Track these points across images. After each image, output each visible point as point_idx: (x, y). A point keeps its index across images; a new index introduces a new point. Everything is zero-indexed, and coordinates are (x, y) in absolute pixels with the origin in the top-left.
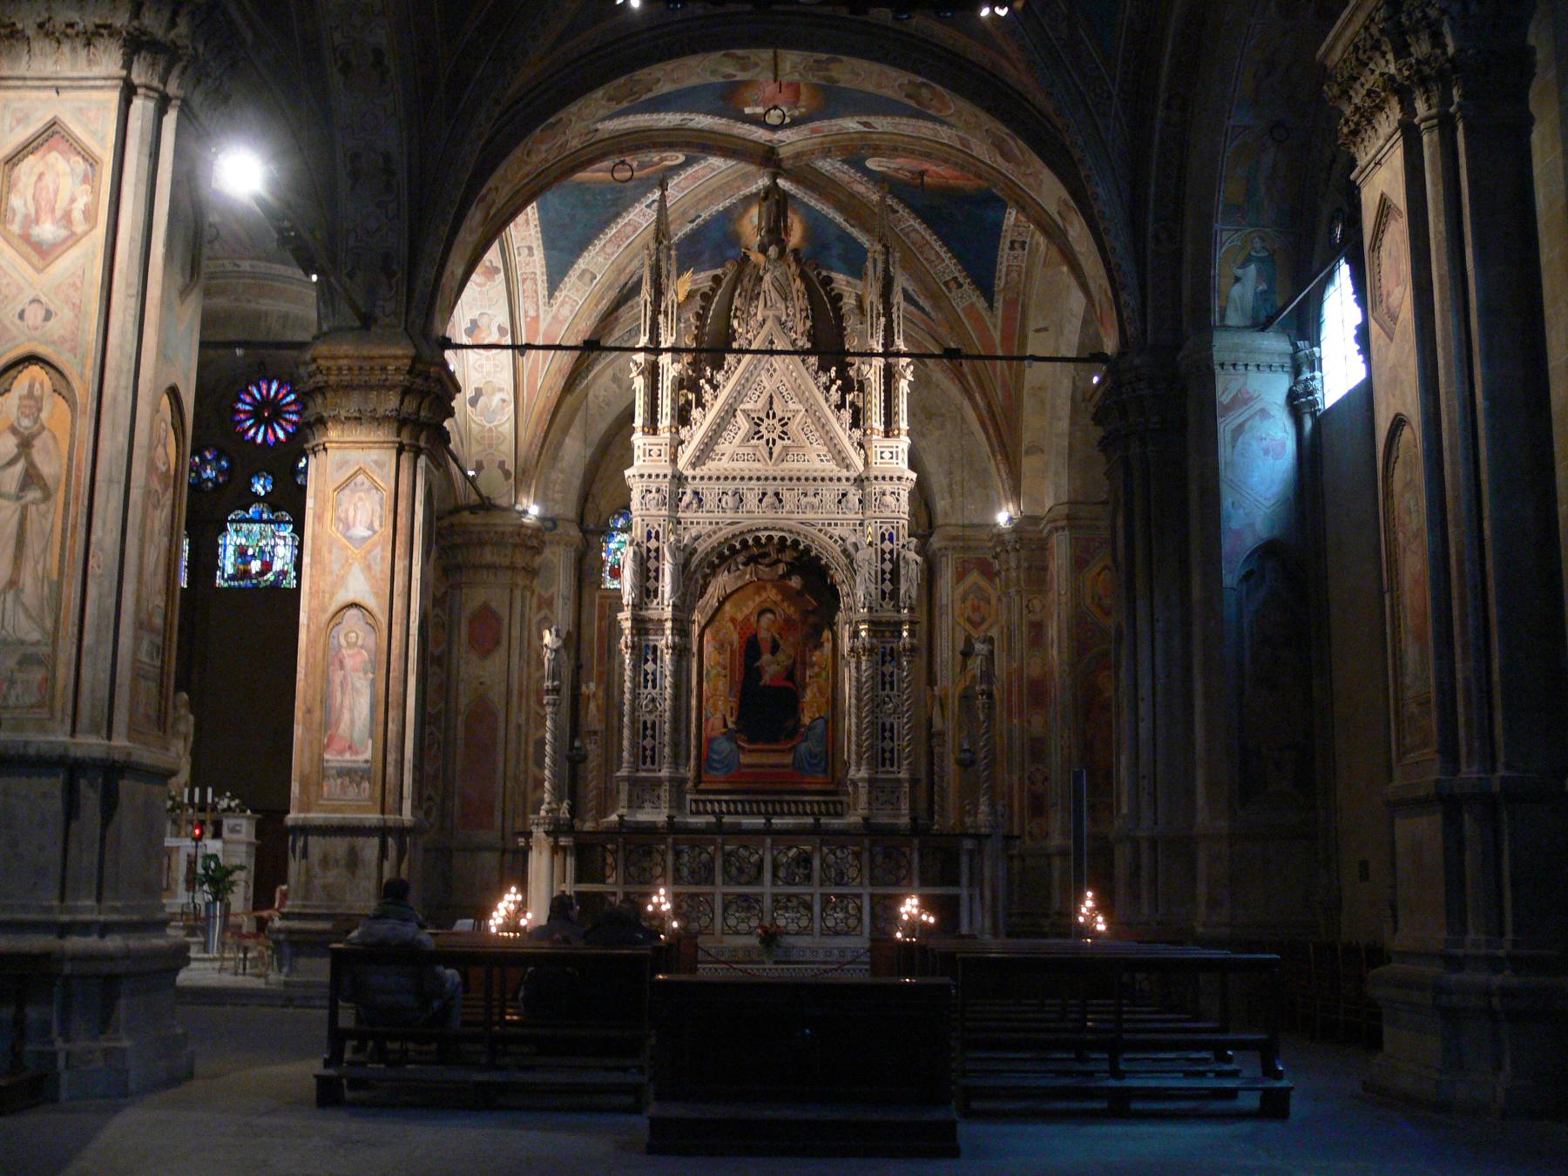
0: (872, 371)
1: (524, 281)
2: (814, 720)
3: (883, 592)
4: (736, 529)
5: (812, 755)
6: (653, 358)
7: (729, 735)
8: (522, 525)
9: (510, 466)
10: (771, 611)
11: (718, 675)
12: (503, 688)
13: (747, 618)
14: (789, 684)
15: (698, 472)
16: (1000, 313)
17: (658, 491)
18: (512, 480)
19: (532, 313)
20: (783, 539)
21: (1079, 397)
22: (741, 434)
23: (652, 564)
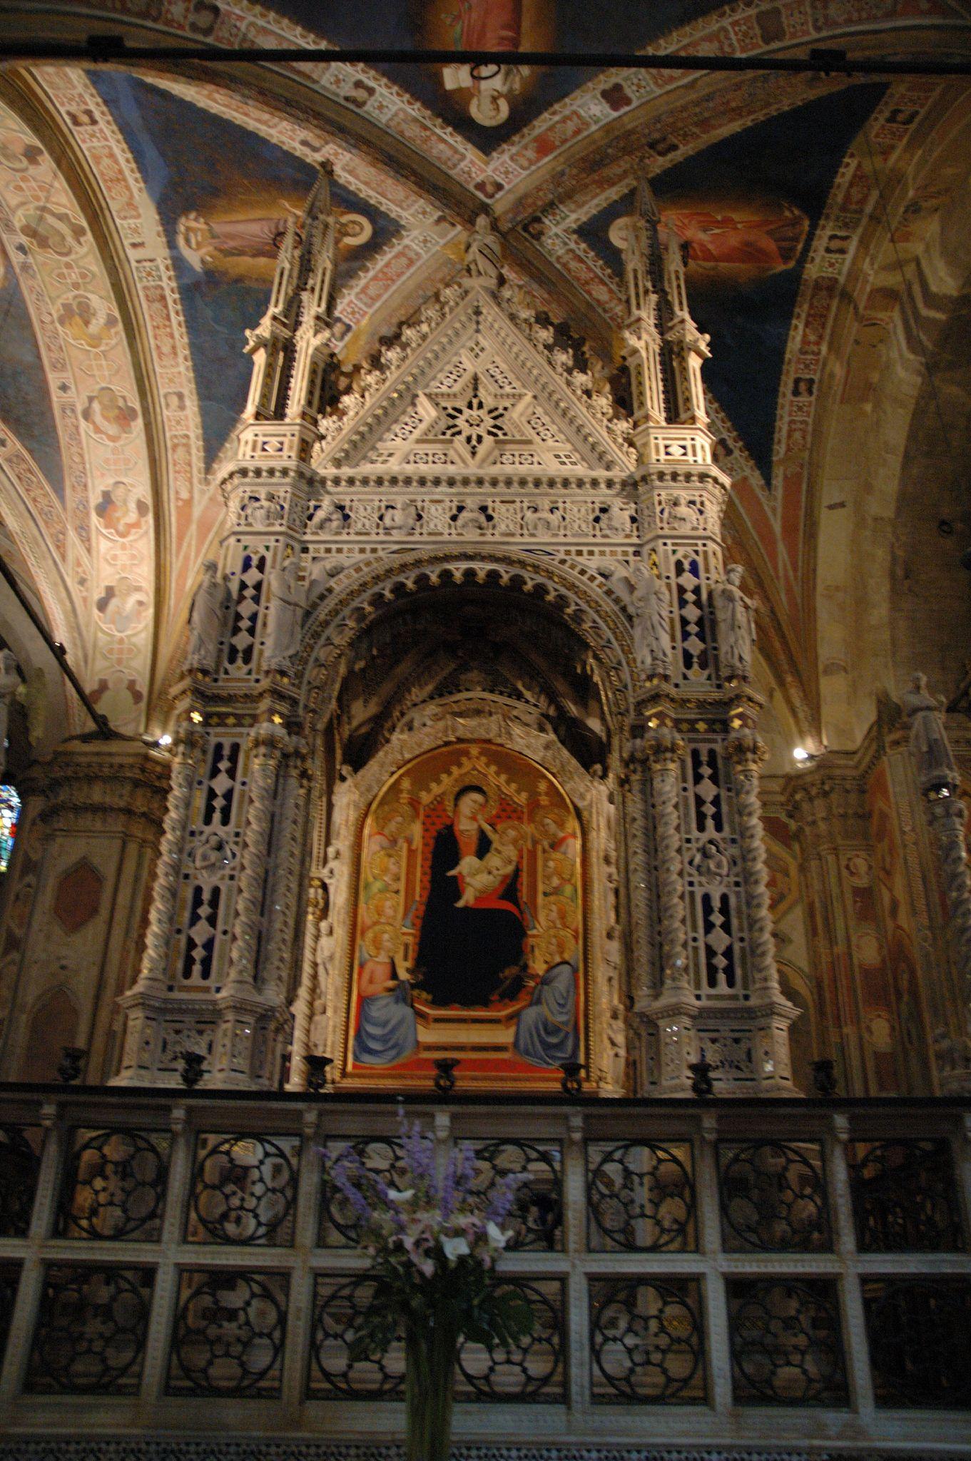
0: (643, 343)
1: (175, 447)
2: (551, 968)
3: (688, 659)
4: (409, 558)
5: (551, 1030)
6: (286, 333)
7: (400, 993)
8: (147, 758)
9: (143, 687)
10: (478, 789)
11: (386, 889)
12: (95, 971)
13: (439, 800)
14: (506, 905)
15: (346, 471)
16: (779, 493)
17: (271, 498)
18: (143, 705)
19: (185, 495)
20: (493, 575)
21: (900, 572)
22: (423, 426)
23: (246, 608)
